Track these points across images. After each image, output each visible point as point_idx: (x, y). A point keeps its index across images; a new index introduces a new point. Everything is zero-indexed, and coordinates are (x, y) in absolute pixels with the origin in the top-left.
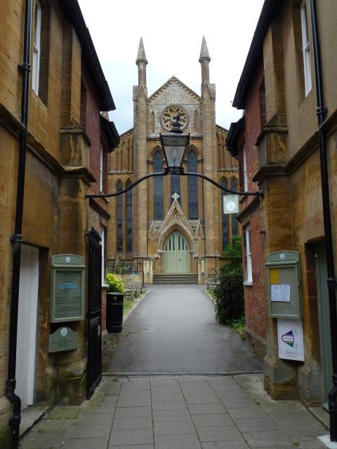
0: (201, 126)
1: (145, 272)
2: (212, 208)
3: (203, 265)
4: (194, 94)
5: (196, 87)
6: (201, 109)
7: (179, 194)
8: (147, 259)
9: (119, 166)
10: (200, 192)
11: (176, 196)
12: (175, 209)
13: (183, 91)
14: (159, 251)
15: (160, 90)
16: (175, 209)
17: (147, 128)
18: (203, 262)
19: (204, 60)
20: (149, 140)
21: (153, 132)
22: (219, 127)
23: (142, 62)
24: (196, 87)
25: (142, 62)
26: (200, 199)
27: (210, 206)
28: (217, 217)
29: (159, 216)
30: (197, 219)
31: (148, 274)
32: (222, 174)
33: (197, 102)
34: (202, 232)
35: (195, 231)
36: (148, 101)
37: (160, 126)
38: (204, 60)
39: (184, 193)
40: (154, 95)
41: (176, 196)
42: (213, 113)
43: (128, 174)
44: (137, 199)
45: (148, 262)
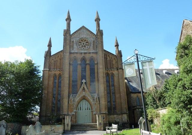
0: (97, 47)
1: (66, 123)
5: (94, 31)
6: (96, 40)
7: (86, 80)
8: (68, 115)
9: (55, 68)
12: (84, 88)
16: (84, 88)
19: (98, 20)
20: (70, 53)
21: (73, 50)
23: (69, 19)
24: (94, 31)
25: (69, 19)
28: (106, 92)
29: (75, 92)
30: (95, 93)
35: (94, 100)
36: (71, 36)
37: (76, 47)
38: (98, 20)
39: (88, 79)
40: (74, 33)
41: (84, 81)
45: (68, 117)
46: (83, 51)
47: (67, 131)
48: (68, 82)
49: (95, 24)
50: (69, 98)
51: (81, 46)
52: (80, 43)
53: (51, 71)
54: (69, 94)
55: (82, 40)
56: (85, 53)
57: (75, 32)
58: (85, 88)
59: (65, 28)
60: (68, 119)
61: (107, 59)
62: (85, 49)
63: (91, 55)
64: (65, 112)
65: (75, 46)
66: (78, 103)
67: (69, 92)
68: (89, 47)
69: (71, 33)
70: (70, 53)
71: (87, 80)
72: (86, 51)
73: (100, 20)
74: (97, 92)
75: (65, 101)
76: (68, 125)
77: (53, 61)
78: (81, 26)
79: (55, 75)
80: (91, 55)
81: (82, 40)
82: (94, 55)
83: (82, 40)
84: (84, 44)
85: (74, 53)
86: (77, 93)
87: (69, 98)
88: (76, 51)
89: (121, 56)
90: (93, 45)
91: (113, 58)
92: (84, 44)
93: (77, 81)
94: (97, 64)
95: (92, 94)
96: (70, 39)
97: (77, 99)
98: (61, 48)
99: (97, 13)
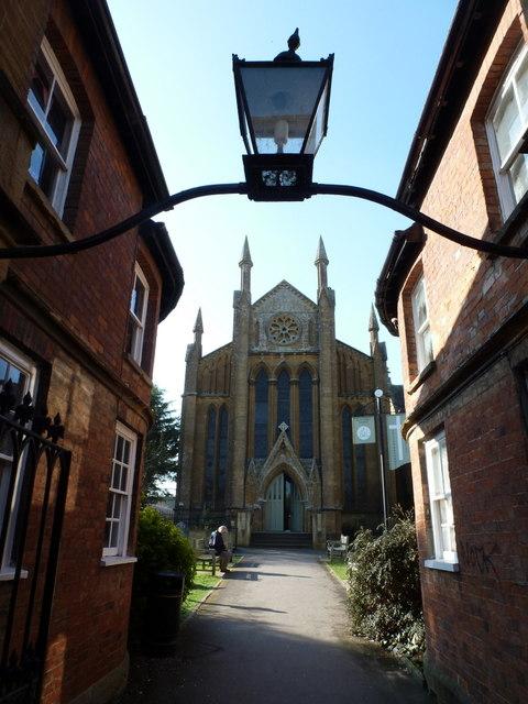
0: (318, 339)
1: (240, 529)
2: (331, 443)
3: (319, 522)
4: (305, 298)
5: (311, 292)
6: (317, 318)
7: (288, 423)
8: (243, 509)
9: (213, 389)
10: (315, 422)
11: (284, 426)
12: (283, 443)
13: (296, 298)
14: (260, 499)
15: (267, 295)
16: (283, 443)
17: (250, 340)
18: (319, 515)
19: (322, 262)
20: (251, 354)
21: (257, 345)
22: (339, 342)
23: (246, 263)
24: (311, 292)
25: (246, 263)
26: (315, 430)
27: (329, 441)
28: (338, 455)
29: (262, 453)
30: (312, 457)
31: (244, 532)
32: (343, 400)
33: (312, 310)
34: (318, 476)
35: (308, 474)
36: (252, 308)
37: (265, 338)
38: (322, 262)
39: (295, 423)
40: (259, 301)
41: (284, 426)
42: (332, 325)
43: (222, 397)
44: (233, 429)
45: (244, 514)
46: (281, 349)
47: (243, 546)
48: (243, 428)
49: (314, 272)
50: (247, 468)
51: (277, 334)
52: (274, 325)
53: (202, 398)
54: (247, 457)
55: (280, 320)
56: (287, 354)
57: (263, 299)
58: (287, 444)
59: (239, 288)
60: (244, 519)
61: (345, 365)
62: (287, 343)
63: (304, 359)
64: (238, 501)
65: (263, 336)
66: (267, 488)
67: (247, 454)
68: (297, 337)
69: (253, 302)
70: (251, 354)
71: (291, 422)
72: (289, 350)
73: (327, 262)
74: (316, 454)
75: (239, 475)
76: (244, 532)
77: (206, 371)
78: (278, 282)
79: (211, 410)
80: (304, 359)
81: (280, 320)
82: (311, 360)
83: (280, 319)
84: (284, 329)
85: (259, 354)
86: (266, 456)
87: (247, 468)
88: (265, 349)
89: (384, 358)
90: (309, 332)
91: (362, 364)
92: (284, 329)
93: (265, 426)
94: (318, 382)
95: (305, 461)
96: (251, 318)
97: (267, 471)
98: (229, 339)
99: (322, 243)
